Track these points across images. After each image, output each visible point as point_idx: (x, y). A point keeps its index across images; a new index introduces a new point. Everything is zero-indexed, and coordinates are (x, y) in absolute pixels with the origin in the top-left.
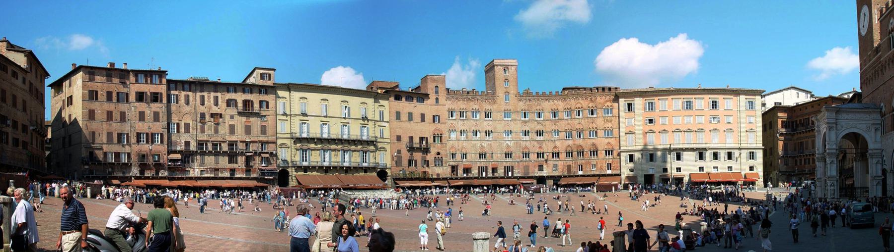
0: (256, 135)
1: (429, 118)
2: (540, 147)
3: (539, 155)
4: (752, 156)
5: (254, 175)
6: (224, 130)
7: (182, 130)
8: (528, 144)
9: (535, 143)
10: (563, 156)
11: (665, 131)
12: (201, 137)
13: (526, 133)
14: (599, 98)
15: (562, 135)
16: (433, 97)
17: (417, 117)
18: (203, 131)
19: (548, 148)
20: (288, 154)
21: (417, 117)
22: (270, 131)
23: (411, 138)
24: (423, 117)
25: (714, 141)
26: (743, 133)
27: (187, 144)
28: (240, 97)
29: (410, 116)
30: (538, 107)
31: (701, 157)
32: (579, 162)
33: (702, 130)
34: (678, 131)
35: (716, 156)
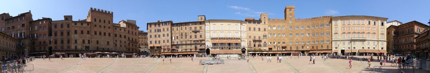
0: (198, 38)
1: (262, 29)
5: (198, 51)
6: (188, 37)
7: (176, 38)
12: (181, 40)
16: (263, 22)
17: (257, 29)
18: (182, 38)
20: (209, 44)
21: (257, 29)
22: (203, 37)
23: (255, 37)
24: (259, 29)
27: (177, 42)
28: (193, 27)
29: (254, 29)
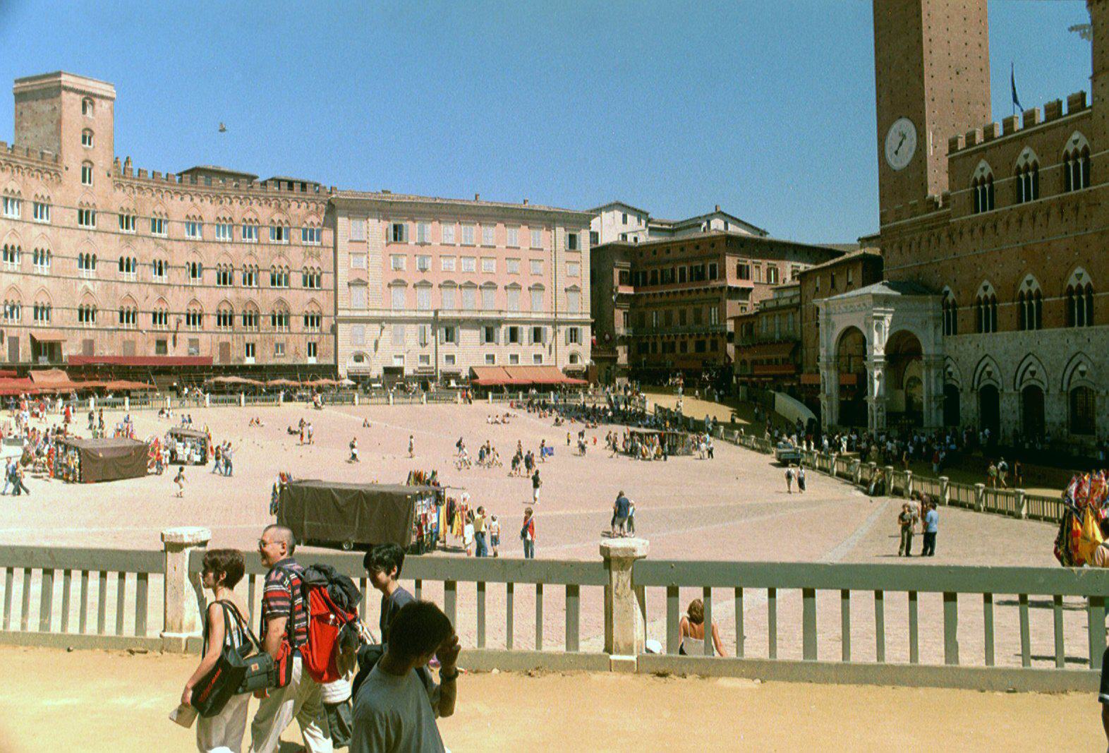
2: (161, 300)
3: (158, 317)
4: (574, 336)
8: (134, 290)
9: (151, 290)
10: (210, 322)
11: (425, 284)
13: (125, 265)
14: (294, 205)
15: (210, 277)
19: (178, 303)
25: (514, 307)
26: (561, 293)
30: (158, 208)
31: (489, 337)
32: (249, 339)
33: (491, 286)
34: (449, 284)
35: (514, 336)
